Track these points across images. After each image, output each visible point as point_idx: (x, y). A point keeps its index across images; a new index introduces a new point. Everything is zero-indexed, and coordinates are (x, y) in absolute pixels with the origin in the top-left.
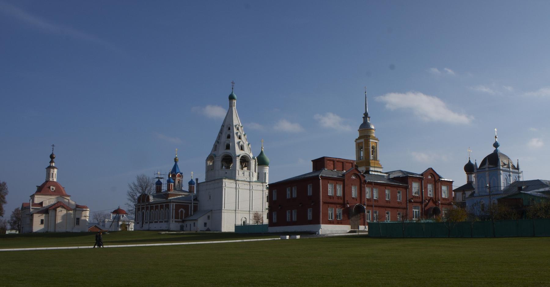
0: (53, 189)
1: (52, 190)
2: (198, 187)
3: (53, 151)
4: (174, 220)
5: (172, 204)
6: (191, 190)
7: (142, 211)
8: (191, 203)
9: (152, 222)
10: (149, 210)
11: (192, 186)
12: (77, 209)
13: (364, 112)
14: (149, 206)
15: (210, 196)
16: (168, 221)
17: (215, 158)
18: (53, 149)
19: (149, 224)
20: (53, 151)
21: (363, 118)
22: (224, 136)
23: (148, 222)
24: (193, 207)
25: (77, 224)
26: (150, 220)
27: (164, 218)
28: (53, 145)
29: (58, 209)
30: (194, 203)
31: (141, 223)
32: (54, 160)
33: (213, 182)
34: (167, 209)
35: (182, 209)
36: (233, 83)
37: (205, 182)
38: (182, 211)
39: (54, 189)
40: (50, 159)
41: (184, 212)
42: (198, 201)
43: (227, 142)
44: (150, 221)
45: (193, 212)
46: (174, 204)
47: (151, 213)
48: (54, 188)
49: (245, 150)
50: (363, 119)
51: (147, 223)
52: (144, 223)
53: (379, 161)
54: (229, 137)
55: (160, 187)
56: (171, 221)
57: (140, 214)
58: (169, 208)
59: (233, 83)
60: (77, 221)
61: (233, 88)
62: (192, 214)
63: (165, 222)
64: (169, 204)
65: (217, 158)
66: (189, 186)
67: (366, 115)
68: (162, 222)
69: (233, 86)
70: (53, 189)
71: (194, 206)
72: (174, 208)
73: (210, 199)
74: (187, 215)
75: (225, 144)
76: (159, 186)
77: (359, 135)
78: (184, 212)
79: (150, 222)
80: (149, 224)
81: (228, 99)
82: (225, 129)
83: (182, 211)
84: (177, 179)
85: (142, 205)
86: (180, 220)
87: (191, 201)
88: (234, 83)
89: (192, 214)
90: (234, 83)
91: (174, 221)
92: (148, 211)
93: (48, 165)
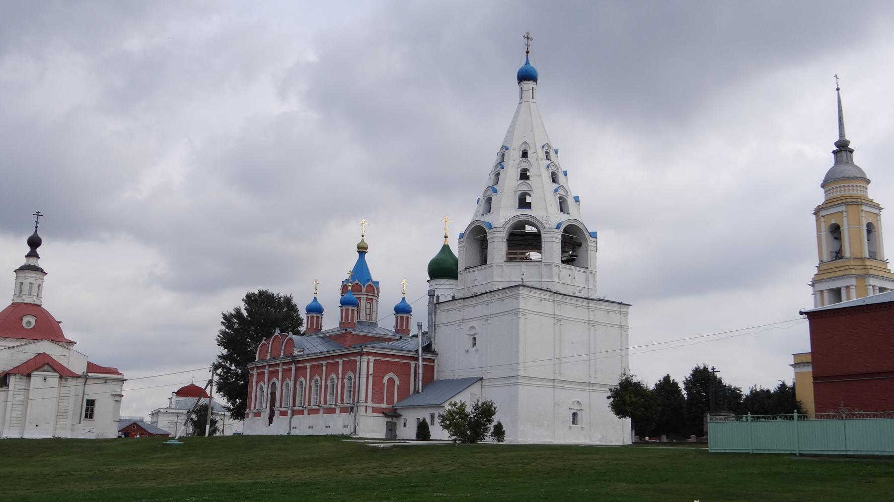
0: (29, 323)
1: (26, 327)
2: (435, 315)
3: (36, 227)
4: (370, 404)
5: (365, 358)
6: (402, 330)
7: (271, 383)
8: (417, 359)
9: (301, 412)
10: (293, 378)
11: (405, 315)
12: (90, 375)
13: (837, 139)
14: (293, 367)
15: (474, 339)
16: (352, 409)
17: (488, 231)
18: (37, 223)
19: (291, 418)
20: (36, 227)
21: (834, 152)
22: (511, 175)
23: (289, 413)
24: (421, 371)
25: (86, 417)
26: (294, 405)
27: (339, 400)
28: (38, 212)
29: (33, 373)
30: (424, 359)
31: (266, 414)
32: (39, 250)
33: (486, 298)
34: (351, 374)
35: (391, 375)
36: (528, 38)
37: (451, 301)
38: (391, 380)
39: (33, 323)
40: (28, 249)
41: (397, 382)
42: (434, 352)
43: (524, 188)
44: (295, 408)
45: (422, 386)
46: (372, 359)
47: (298, 386)
48: (33, 320)
49: (571, 211)
50: (833, 155)
51: (284, 413)
52: (277, 414)
53: (885, 262)
54: (524, 176)
55: (318, 317)
56: (362, 409)
57: (265, 388)
58: (354, 372)
59: (528, 38)
60: (87, 410)
61: (527, 52)
62: (420, 391)
63: (344, 410)
64: (358, 358)
65: (495, 230)
66: (397, 318)
67: (842, 149)
68: (316, 412)
69: (528, 46)
70: (29, 323)
71: (424, 366)
72: (371, 372)
73: (474, 345)
74: (404, 393)
75: (518, 193)
76: (315, 315)
77: (825, 196)
78: (397, 382)
79: (294, 413)
80: (291, 418)
81: (517, 81)
82: (514, 155)
83: (391, 380)
84: (365, 297)
85: (270, 366)
86: (385, 406)
87: (417, 351)
88: (531, 39)
89: (420, 391)
90: (531, 39)
91: (370, 410)
92: (288, 380)
93: (23, 261)
